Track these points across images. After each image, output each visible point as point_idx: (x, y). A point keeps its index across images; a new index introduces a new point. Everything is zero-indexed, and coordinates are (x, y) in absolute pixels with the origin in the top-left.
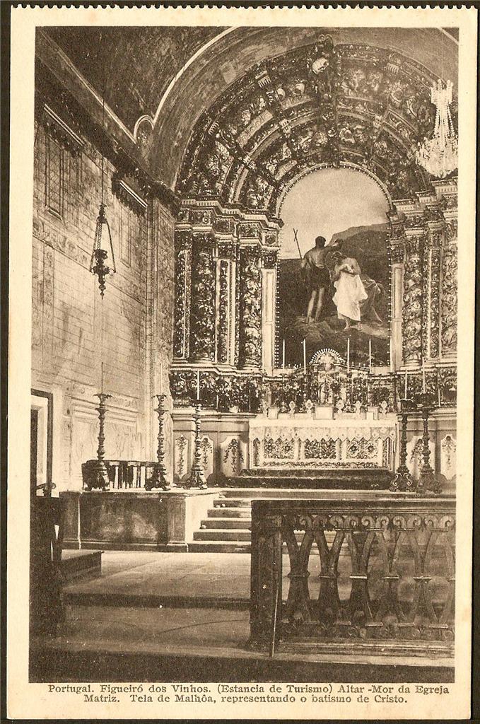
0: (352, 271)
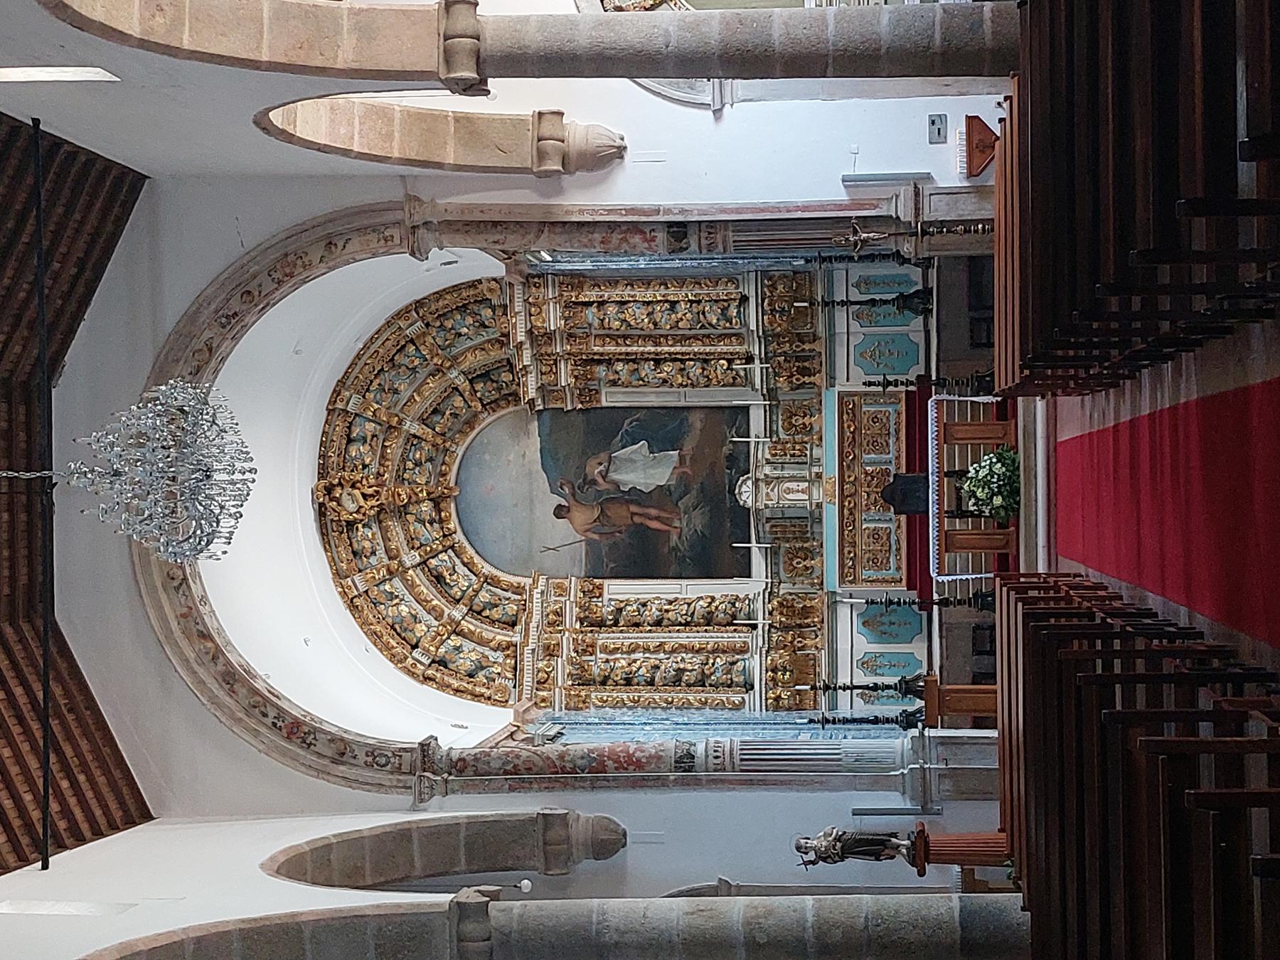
0: (606, 464)
